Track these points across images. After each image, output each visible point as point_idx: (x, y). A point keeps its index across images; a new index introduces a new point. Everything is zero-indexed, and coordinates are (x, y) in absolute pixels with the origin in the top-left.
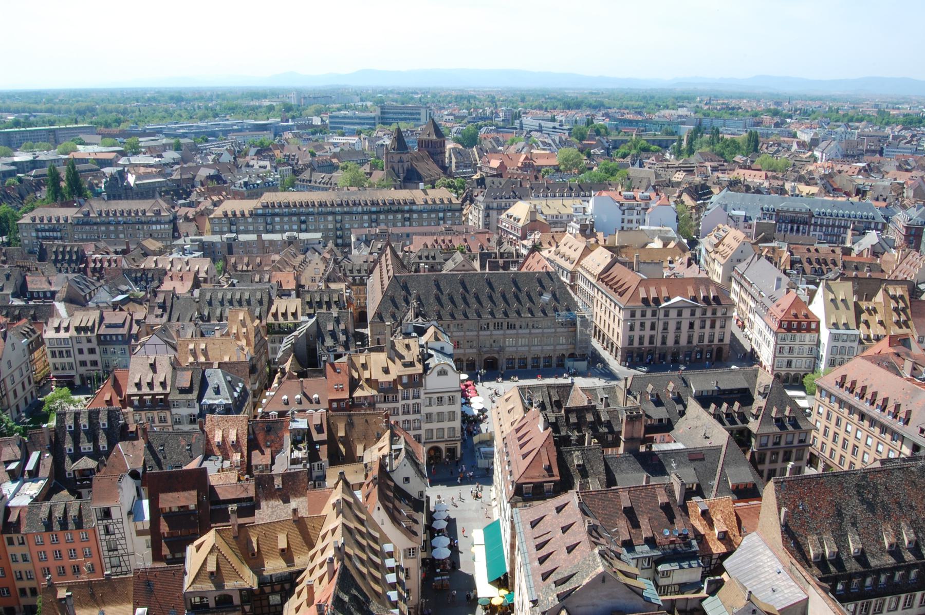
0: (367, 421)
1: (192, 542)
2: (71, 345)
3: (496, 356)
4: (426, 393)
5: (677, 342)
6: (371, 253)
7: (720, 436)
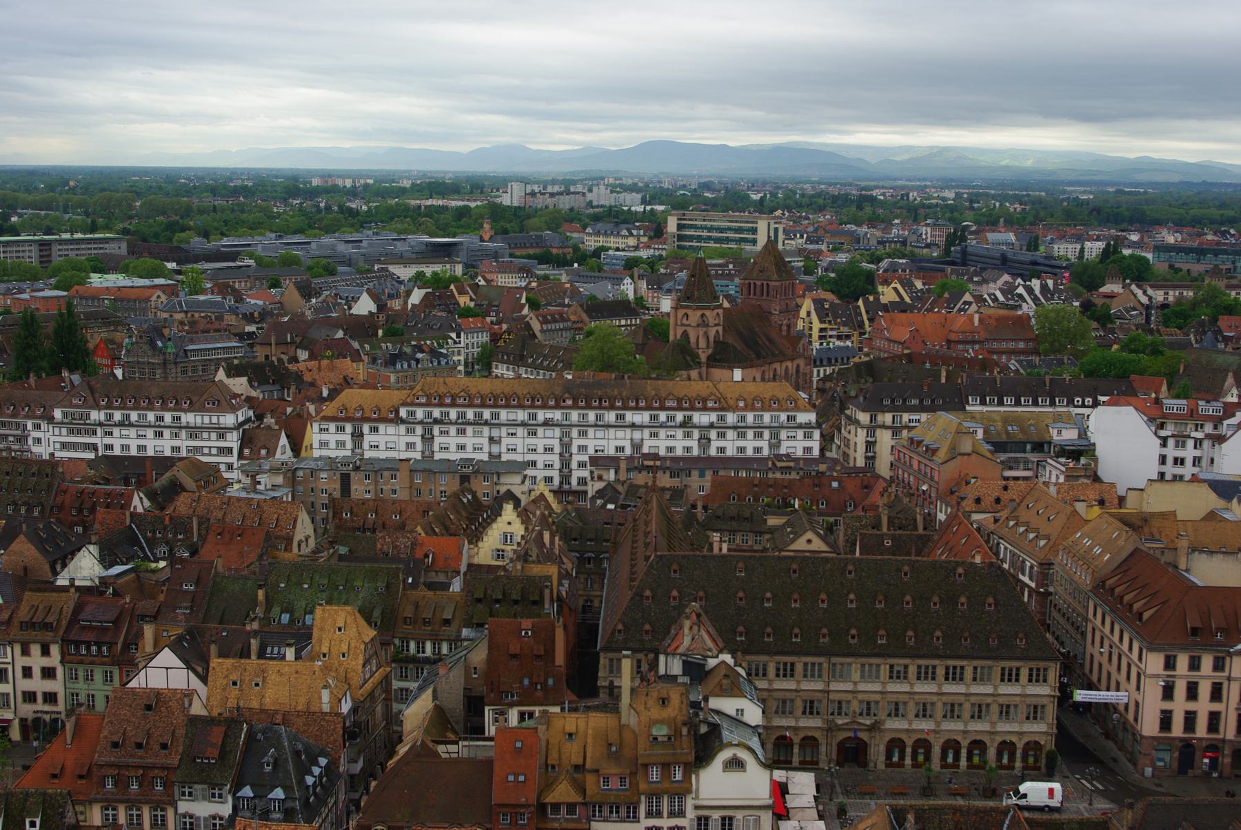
2: (9, 659)
3: (864, 736)
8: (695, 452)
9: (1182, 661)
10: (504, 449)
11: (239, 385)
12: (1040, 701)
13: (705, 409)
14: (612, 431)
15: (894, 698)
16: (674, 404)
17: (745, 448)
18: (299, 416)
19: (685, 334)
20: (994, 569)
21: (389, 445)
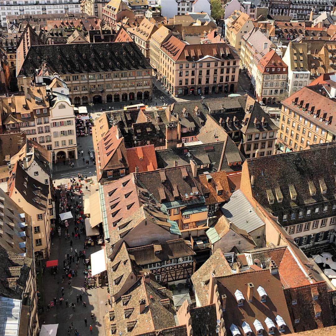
3: (100, 94)
4: (52, 120)
5: (207, 82)
6: (20, 32)
7: (223, 136)
14: (13, 7)
17: (57, 11)
20: (132, 45)
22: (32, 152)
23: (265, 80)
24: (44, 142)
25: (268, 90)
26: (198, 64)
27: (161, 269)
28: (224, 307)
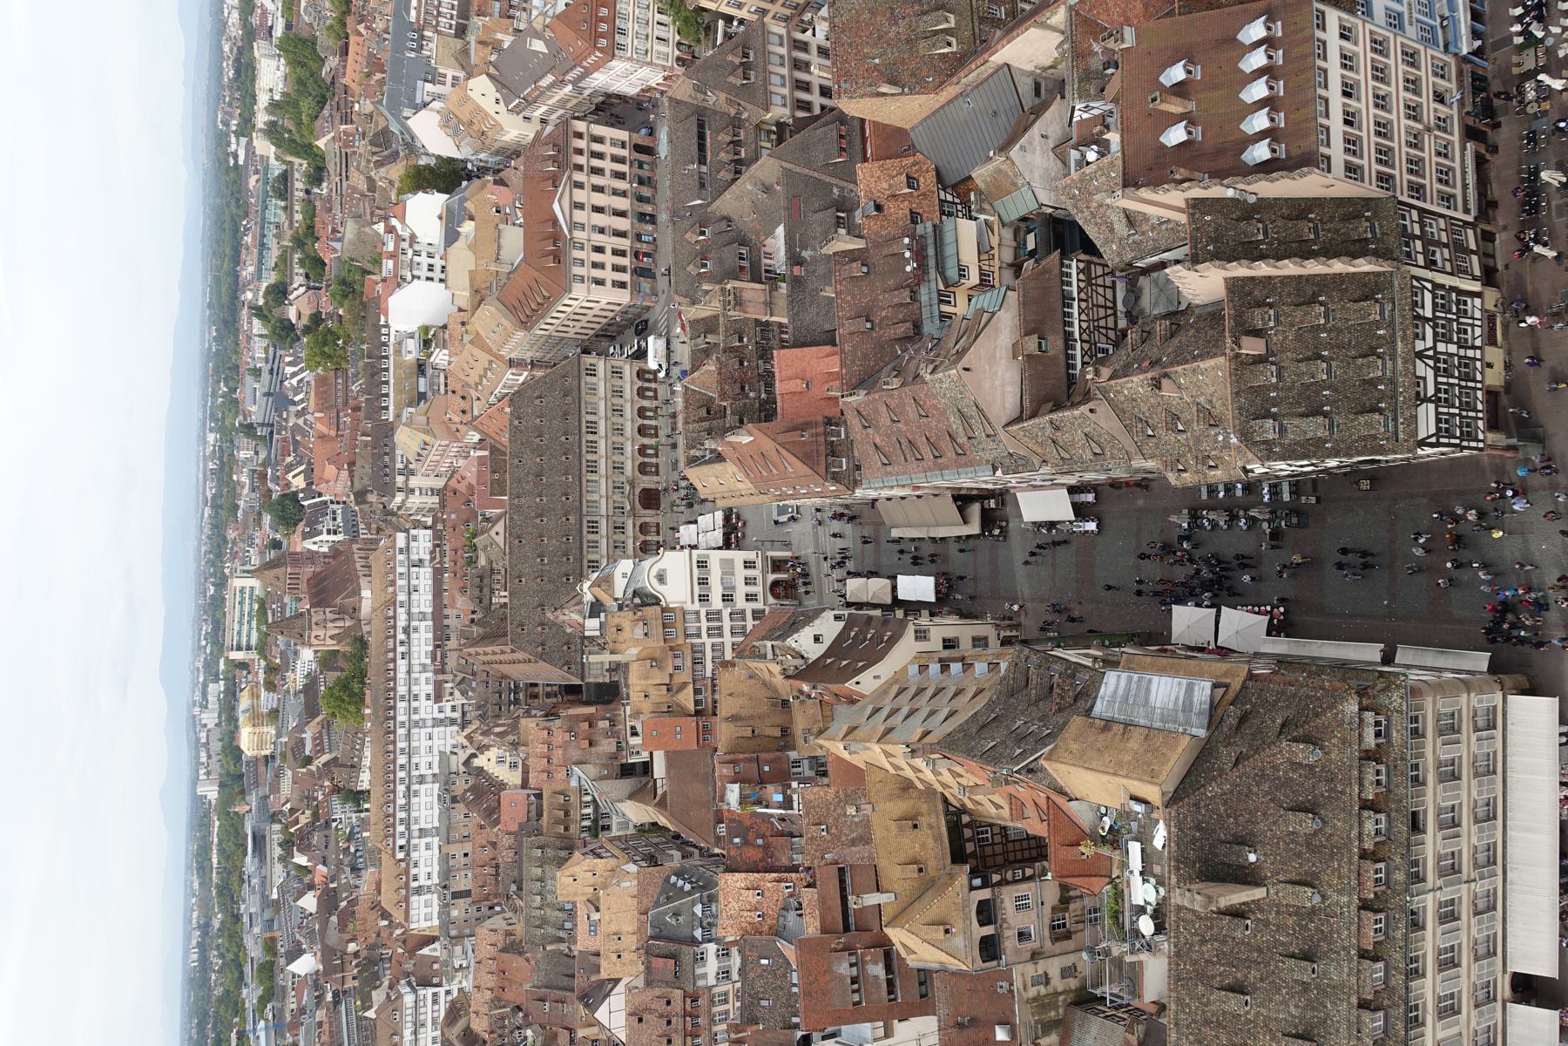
0: (730, 695)
1: (904, 959)
3: (638, 491)
5: (622, 214)
8: (431, 623)
9: (577, 270)
10: (430, 772)
11: (378, 996)
12: (609, 369)
13: (394, 617)
15: (610, 470)
16: (391, 643)
18: (404, 942)
19: (332, 637)
20: (516, 398)
21: (429, 863)
22: (765, 646)
23: (629, 55)
24: (744, 627)
25: (655, 47)
26: (578, 234)
27: (1082, 341)
28: (1197, 175)
